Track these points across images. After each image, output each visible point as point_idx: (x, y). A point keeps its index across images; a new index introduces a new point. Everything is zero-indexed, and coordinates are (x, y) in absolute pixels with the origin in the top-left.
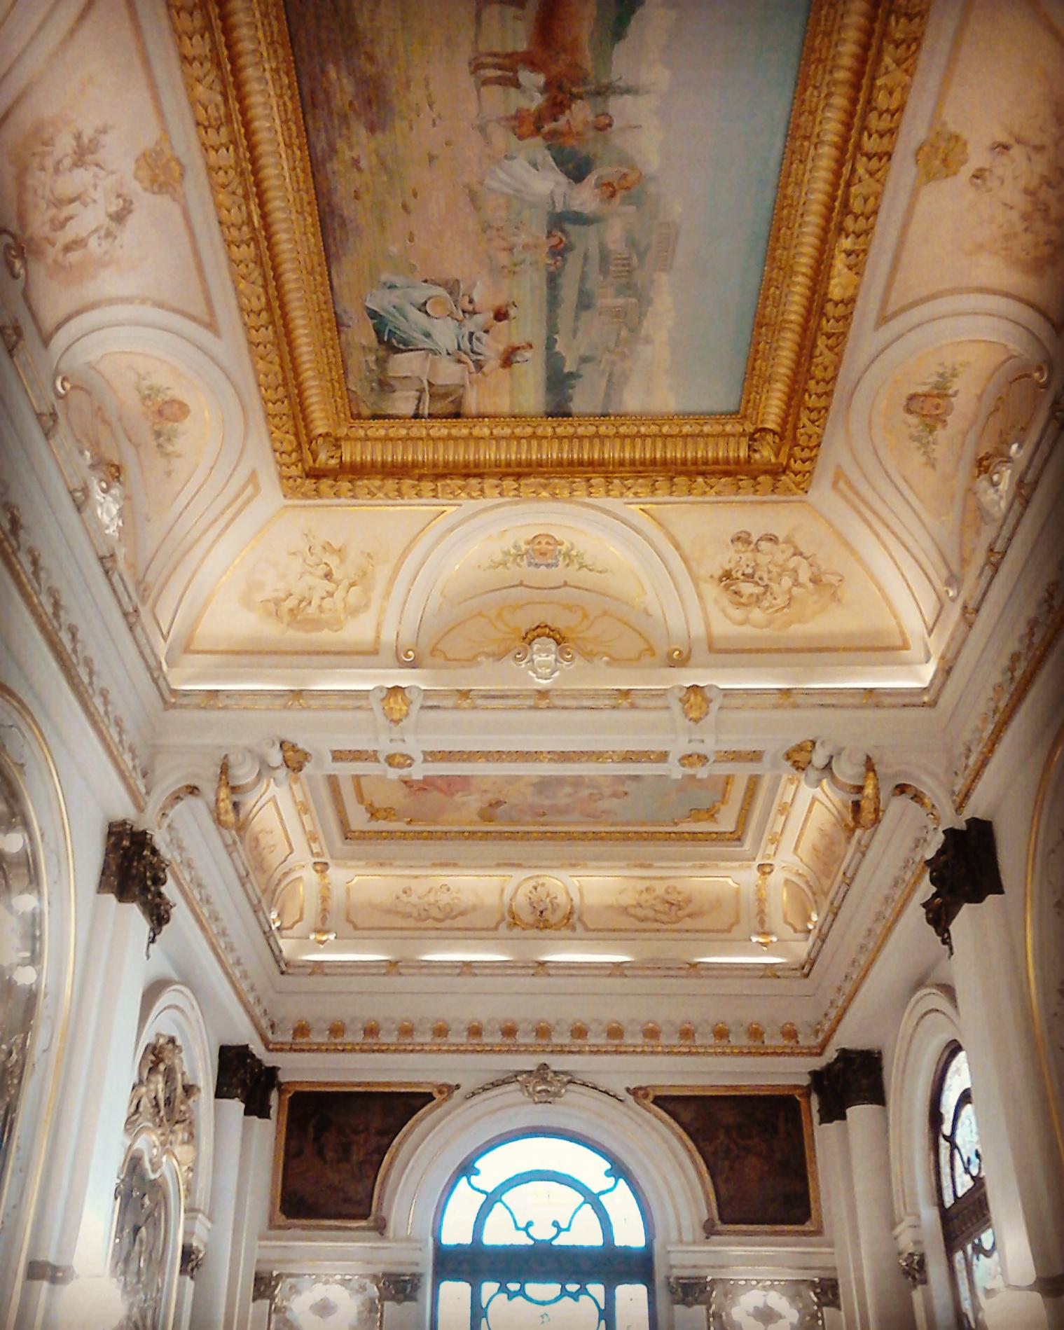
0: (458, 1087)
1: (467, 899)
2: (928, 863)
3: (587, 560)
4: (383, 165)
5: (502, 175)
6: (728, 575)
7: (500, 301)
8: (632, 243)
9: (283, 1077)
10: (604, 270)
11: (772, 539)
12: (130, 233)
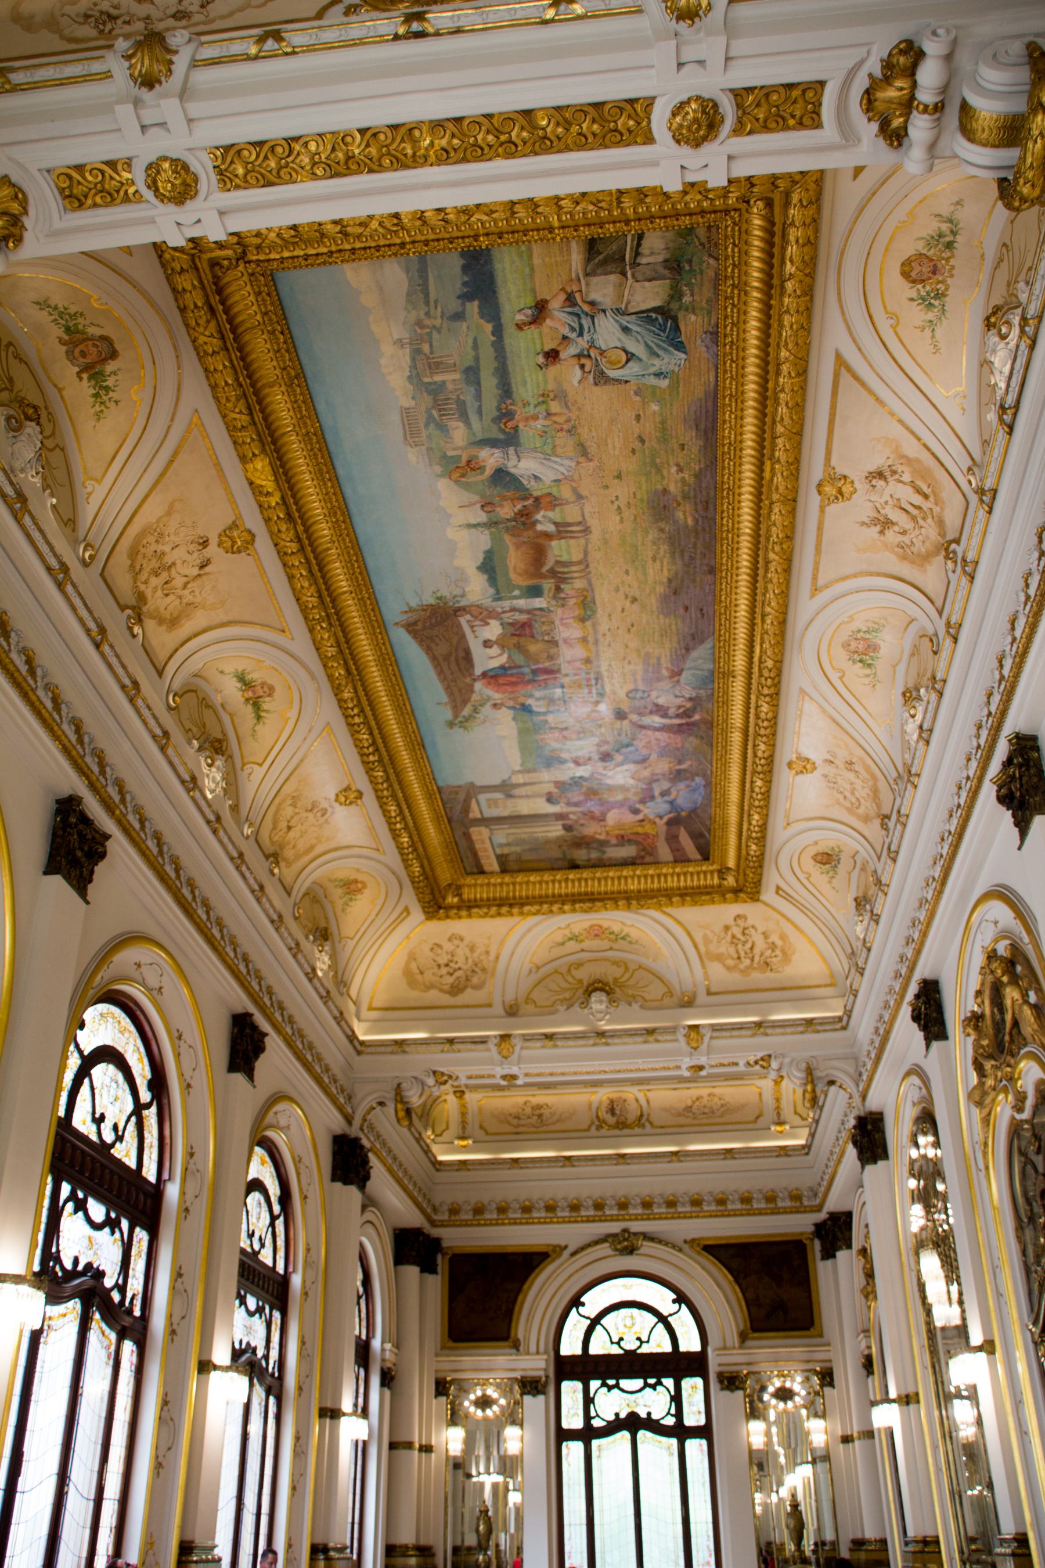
4: (659, 470)
5: (562, 469)
7: (553, 370)
8: (442, 428)
12: (878, 461)
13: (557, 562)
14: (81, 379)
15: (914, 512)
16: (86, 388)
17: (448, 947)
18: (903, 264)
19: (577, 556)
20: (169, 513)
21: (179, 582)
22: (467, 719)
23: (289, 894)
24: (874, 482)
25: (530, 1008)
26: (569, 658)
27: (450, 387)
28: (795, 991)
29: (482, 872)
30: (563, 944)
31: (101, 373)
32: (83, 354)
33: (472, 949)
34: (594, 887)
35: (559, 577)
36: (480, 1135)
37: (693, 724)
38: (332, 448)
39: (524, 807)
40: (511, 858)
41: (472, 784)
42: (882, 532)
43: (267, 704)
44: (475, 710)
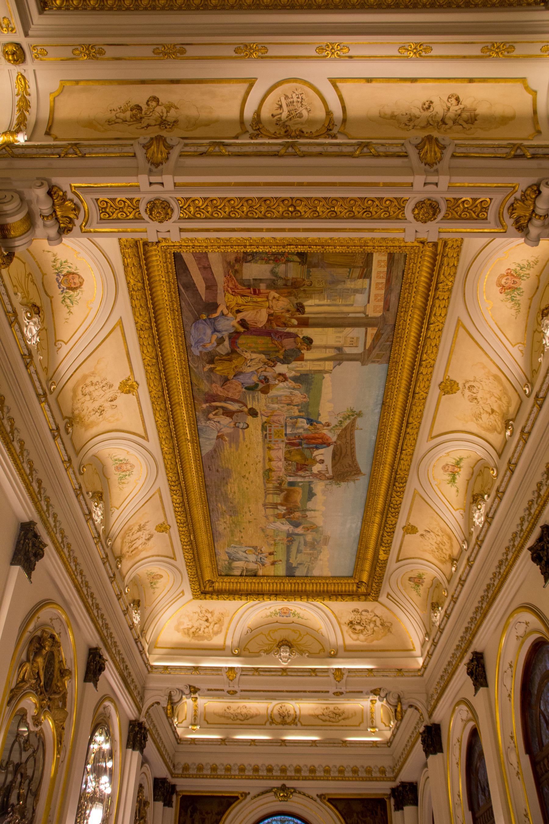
0: (249, 793)
1: (253, 711)
2: (421, 734)
3: (301, 615)
6: (351, 622)
7: (271, 551)
9: (178, 789)
11: (367, 611)
13: (279, 495)
20: (425, 551)
22: (348, 417)
26: (281, 451)
35: (279, 489)
37: (207, 401)
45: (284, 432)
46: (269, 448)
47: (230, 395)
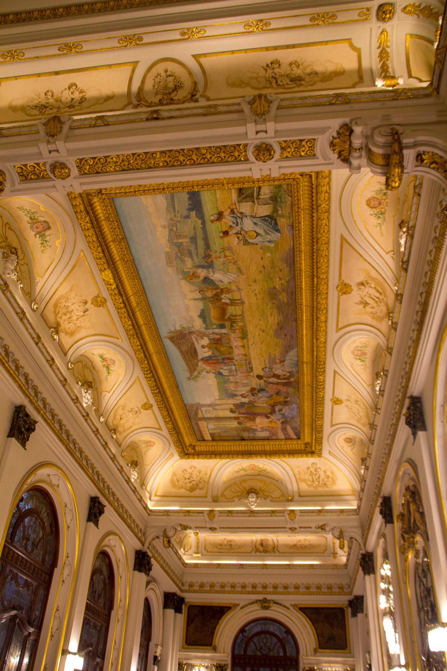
4: (271, 279)
7: (226, 239)
8: (182, 260)
10: (190, 251)
12: (361, 278)
13: (231, 315)
14: (36, 237)
15: (377, 300)
16: (38, 240)
17: (189, 471)
18: (367, 201)
19: (239, 313)
21: (75, 318)
22: (196, 377)
23: (120, 446)
24: (360, 287)
25: (223, 499)
26: (237, 353)
27: (185, 244)
28: (336, 497)
29: (204, 440)
30: (238, 472)
31: (44, 235)
32: (37, 227)
33: (200, 472)
34: (252, 448)
35: (232, 321)
36: (204, 552)
37: (291, 382)
38: (138, 267)
39: (221, 414)
40: (216, 435)
41: (199, 404)
42: (364, 307)
43: (112, 368)
44: (199, 373)
45: (237, 366)
46: (245, 355)
47: (275, 386)
